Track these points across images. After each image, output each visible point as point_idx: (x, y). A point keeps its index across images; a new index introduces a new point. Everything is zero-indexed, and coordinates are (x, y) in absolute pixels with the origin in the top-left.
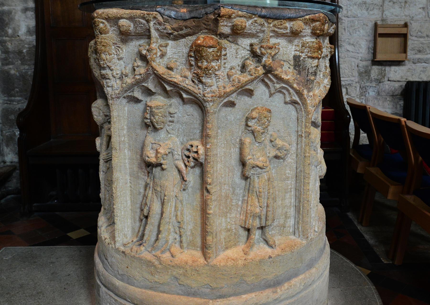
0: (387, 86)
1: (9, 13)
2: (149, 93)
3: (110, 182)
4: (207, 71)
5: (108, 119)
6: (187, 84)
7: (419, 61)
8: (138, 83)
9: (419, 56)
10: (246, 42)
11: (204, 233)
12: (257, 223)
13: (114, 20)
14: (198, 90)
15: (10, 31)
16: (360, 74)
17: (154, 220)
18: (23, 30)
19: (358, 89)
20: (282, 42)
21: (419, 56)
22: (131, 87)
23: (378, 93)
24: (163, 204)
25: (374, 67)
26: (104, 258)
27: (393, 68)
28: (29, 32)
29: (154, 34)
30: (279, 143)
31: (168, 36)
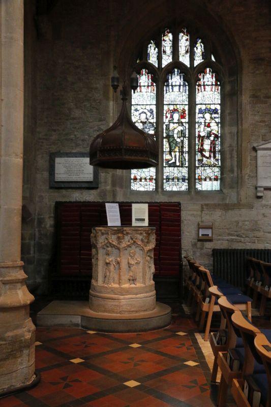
0: (205, 251)
1: (43, 218)
2: (108, 247)
3: (97, 271)
4: (121, 242)
5: (97, 254)
6: (116, 244)
7: (219, 240)
8: (105, 244)
9: (219, 237)
10: (130, 235)
11: (120, 279)
12: (132, 278)
13: (101, 230)
14: (118, 246)
15: (43, 226)
16: (193, 245)
17: (107, 277)
18: (48, 226)
19: (192, 252)
20: (138, 235)
21: (219, 237)
22: (103, 246)
23: (201, 254)
24: (110, 273)
25: (199, 242)
26: (95, 290)
27: (207, 243)
28: (51, 226)
29: (109, 234)
30: (138, 259)
31: (112, 234)
